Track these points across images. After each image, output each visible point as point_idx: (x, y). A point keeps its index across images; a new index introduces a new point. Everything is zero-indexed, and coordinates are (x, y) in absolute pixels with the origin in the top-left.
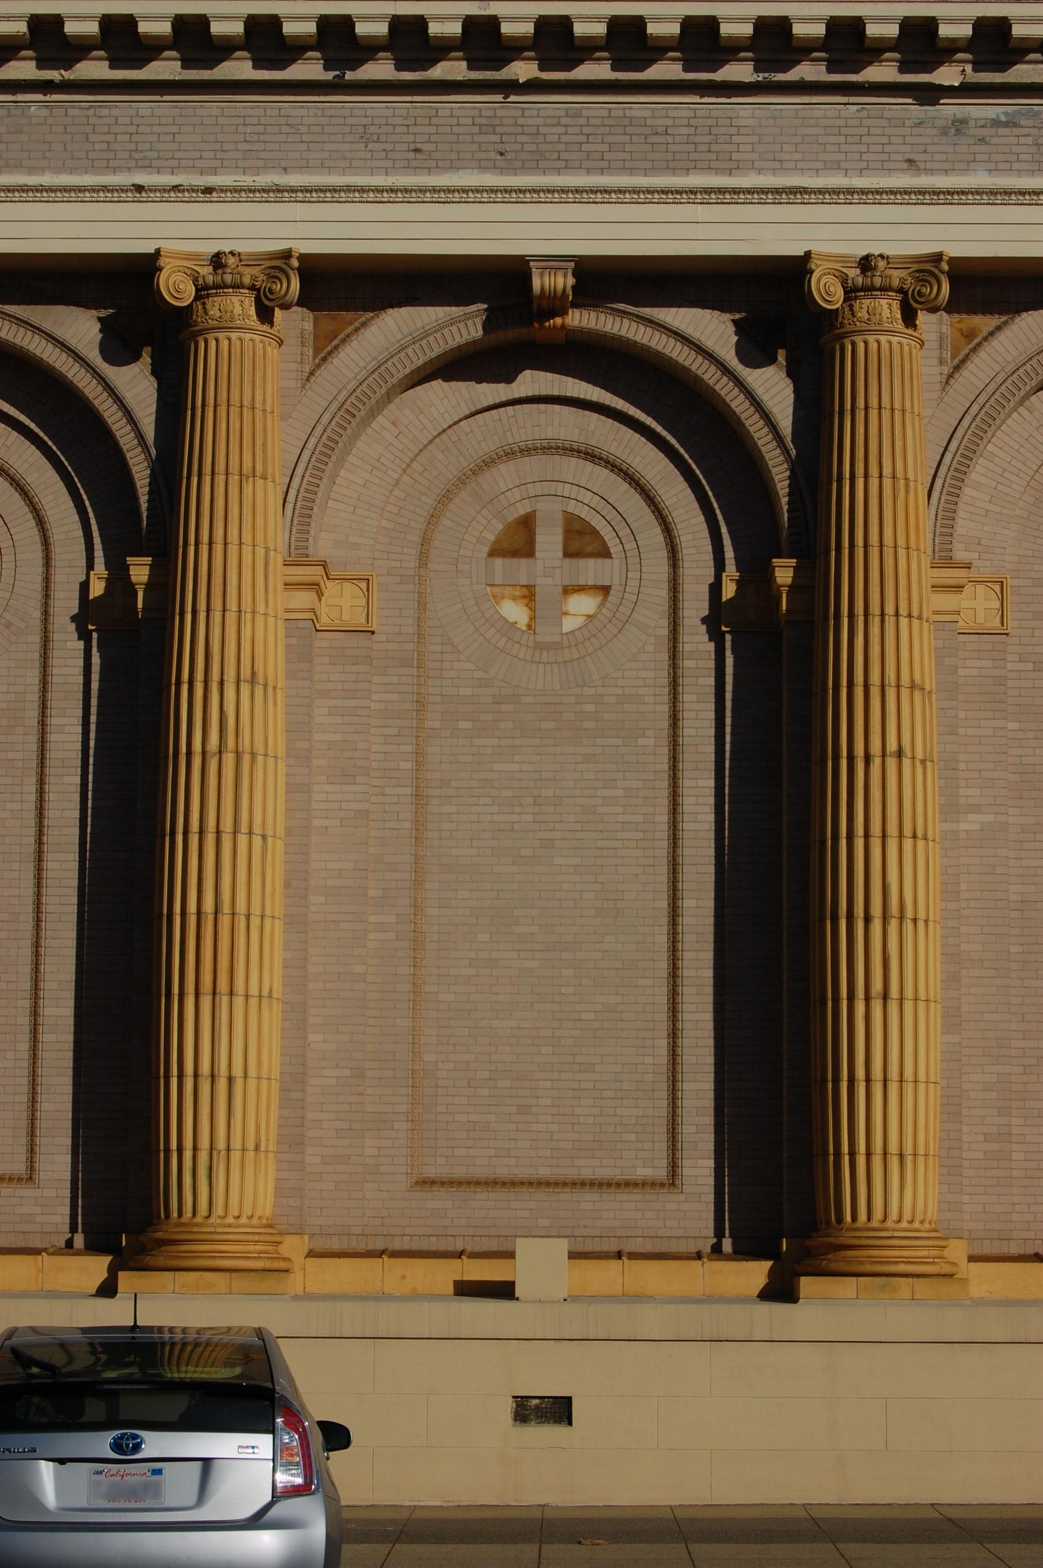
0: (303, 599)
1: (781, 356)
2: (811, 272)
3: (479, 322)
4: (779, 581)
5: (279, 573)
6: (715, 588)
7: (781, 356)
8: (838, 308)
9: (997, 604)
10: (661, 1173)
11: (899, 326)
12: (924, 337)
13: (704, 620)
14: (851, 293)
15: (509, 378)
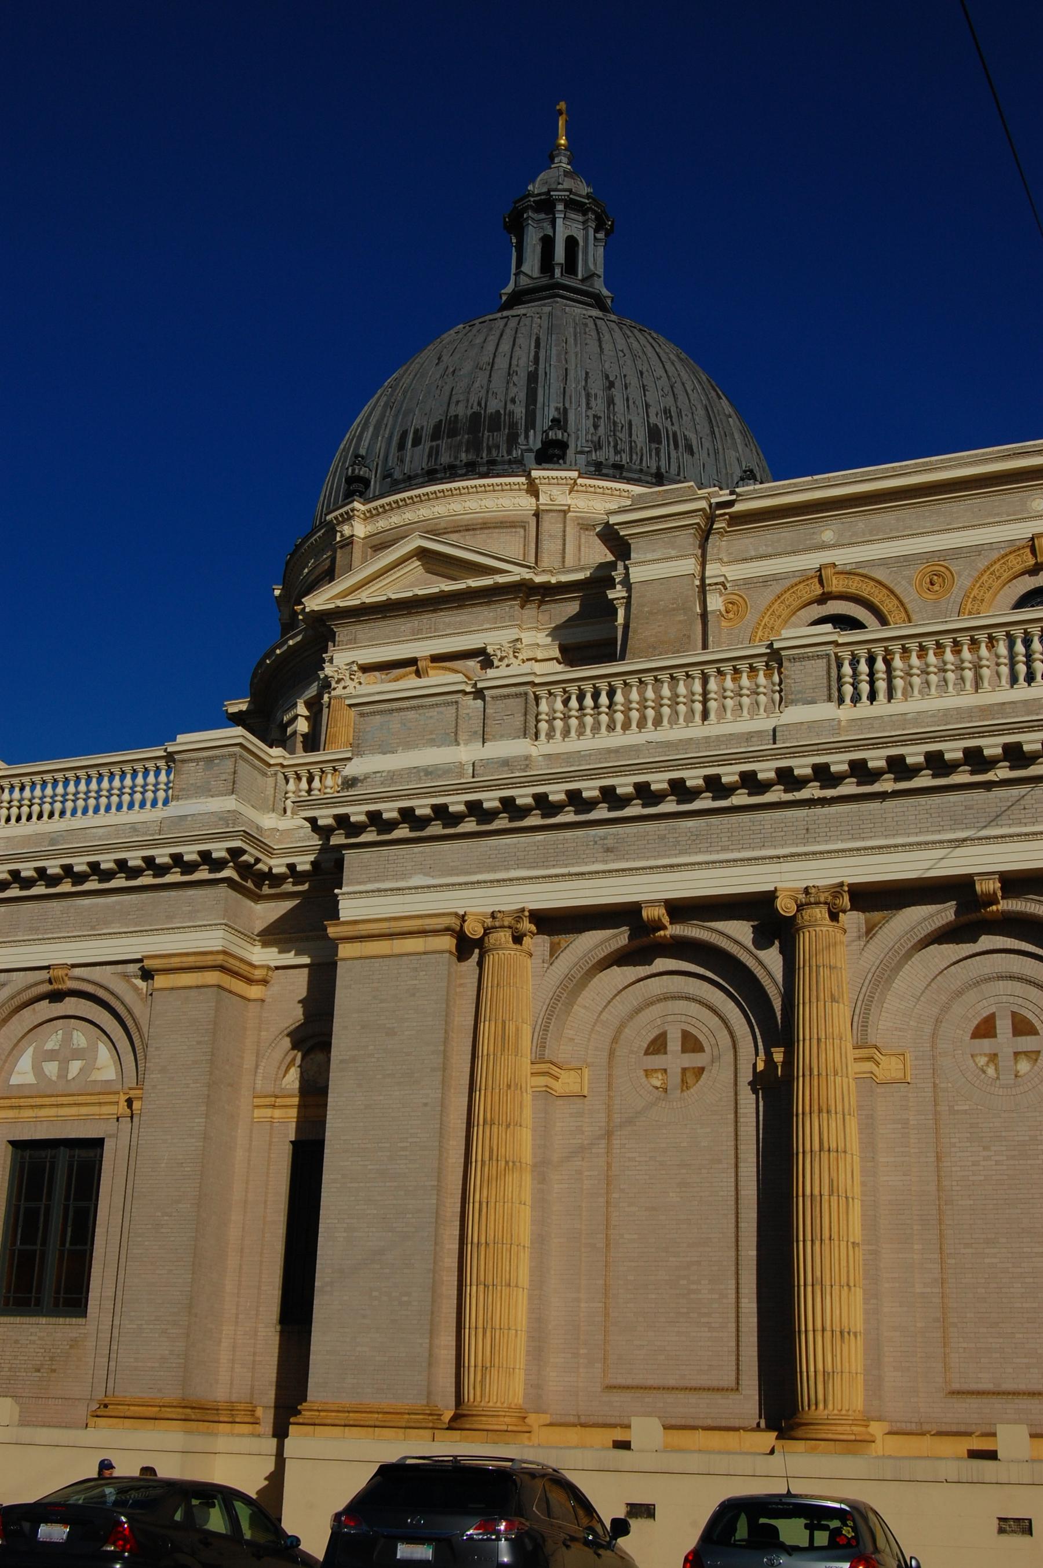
0: (542, 1080)
1: (777, 943)
2: (777, 897)
3: (626, 935)
4: (776, 1060)
5: (526, 1067)
6: (755, 1065)
7: (777, 943)
8: (795, 915)
9: (902, 1066)
10: (733, 1384)
11: (827, 921)
12: (846, 927)
13: (750, 1083)
14: (800, 907)
15: (650, 963)
